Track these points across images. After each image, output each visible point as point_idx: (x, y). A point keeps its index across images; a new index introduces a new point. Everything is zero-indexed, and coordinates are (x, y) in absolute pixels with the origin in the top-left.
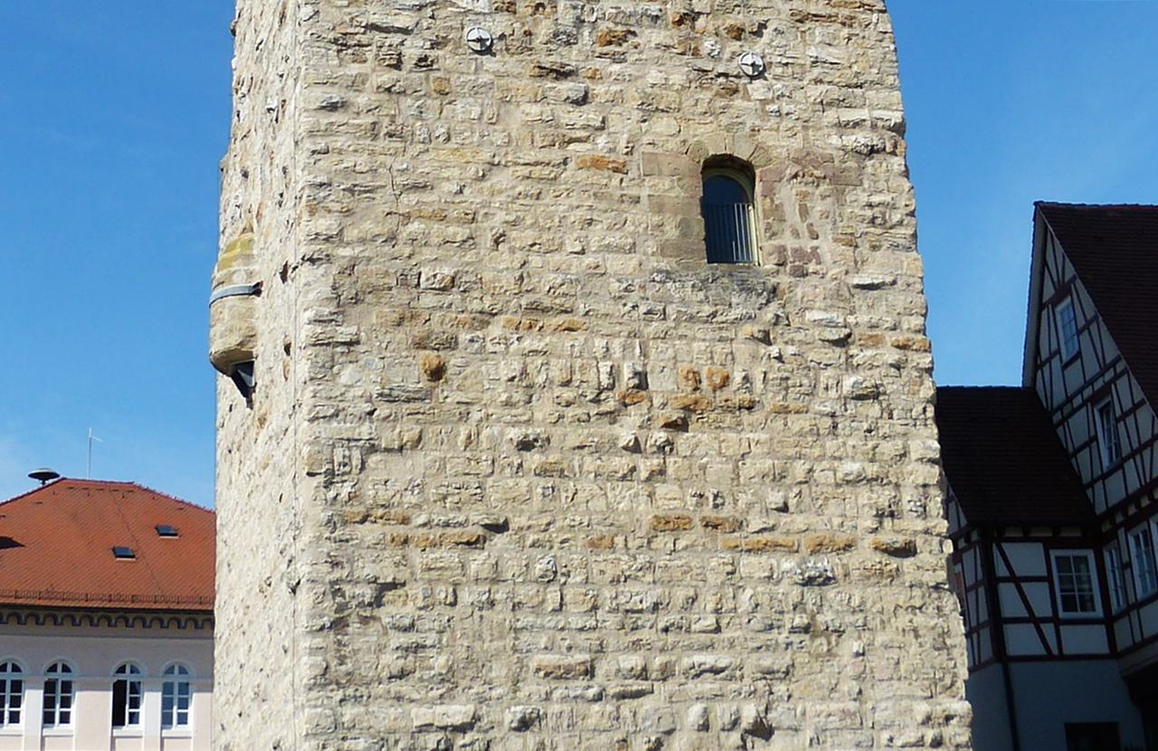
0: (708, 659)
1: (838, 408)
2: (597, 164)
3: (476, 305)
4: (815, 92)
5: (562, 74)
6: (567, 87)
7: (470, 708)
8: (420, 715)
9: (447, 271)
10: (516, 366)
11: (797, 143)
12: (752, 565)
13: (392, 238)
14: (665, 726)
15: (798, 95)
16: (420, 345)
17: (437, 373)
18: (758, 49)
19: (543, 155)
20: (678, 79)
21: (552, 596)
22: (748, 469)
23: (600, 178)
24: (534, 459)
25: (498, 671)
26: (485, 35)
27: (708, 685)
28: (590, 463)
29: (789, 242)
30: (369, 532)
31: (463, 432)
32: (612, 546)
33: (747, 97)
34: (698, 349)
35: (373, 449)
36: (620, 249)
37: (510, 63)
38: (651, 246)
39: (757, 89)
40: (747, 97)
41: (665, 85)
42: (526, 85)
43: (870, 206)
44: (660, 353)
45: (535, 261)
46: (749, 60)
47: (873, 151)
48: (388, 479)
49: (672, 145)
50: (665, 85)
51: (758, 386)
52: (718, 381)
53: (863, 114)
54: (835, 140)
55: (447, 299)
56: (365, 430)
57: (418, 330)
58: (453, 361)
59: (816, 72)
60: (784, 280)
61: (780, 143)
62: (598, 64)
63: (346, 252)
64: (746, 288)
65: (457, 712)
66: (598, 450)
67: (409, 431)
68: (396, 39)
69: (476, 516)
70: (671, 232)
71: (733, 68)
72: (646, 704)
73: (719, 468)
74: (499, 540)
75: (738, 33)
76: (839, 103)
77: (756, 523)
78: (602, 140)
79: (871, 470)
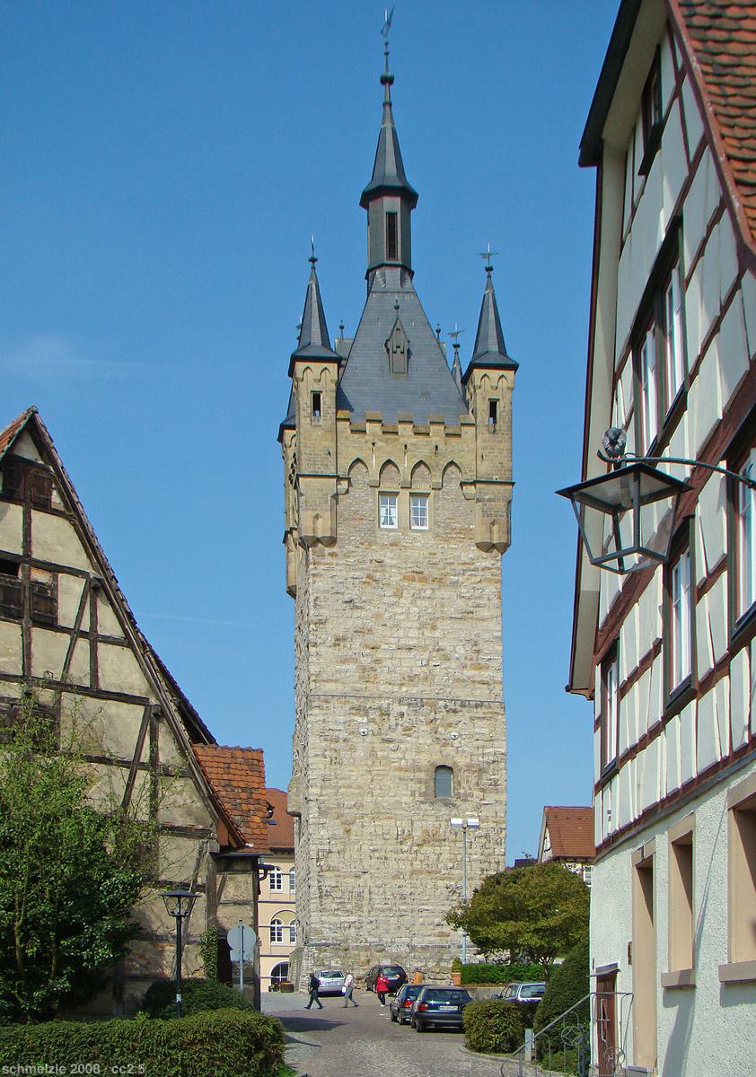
0: (426, 907)
1: (473, 840)
2: (401, 769)
3: (360, 812)
4: (476, 743)
5: (389, 741)
6: (391, 745)
7: (357, 918)
8: (342, 919)
9: (353, 803)
10: (373, 829)
11: (468, 761)
12: (440, 883)
13: (336, 794)
14: (412, 923)
15: (470, 745)
16: (344, 823)
17: (348, 831)
18: (457, 730)
19: (383, 768)
20: (429, 741)
21: (381, 890)
22: (441, 858)
23: (402, 774)
24: (377, 854)
25: (365, 909)
26: (365, 730)
27: (425, 914)
28: (395, 856)
29: (462, 791)
30: (328, 874)
31: (357, 847)
32: (399, 878)
33: (452, 746)
34: (430, 824)
35: (330, 852)
36: (406, 795)
37: (375, 739)
38: (417, 794)
39: (456, 743)
40: (452, 746)
41: (425, 743)
42: (378, 746)
43: (491, 779)
44: (417, 824)
45: (380, 799)
46: (453, 734)
47: (494, 762)
48: (334, 860)
49: (426, 763)
50: (425, 743)
51: (448, 834)
52: (435, 832)
53: (491, 750)
54: (481, 759)
55: (351, 811)
56: (327, 847)
57: (343, 819)
58: (354, 828)
59: (477, 737)
60: (458, 802)
61: (461, 761)
62: (403, 738)
63: (322, 798)
64: (446, 805)
65: (352, 918)
66: (396, 852)
67: (340, 847)
68: (337, 733)
69: (360, 869)
70: (423, 789)
71: (448, 736)
72: (407, 918)
73: (434, 857)
74: (366, 875)
75: (450, 725)
76: (483, 747)
77: (443, 871)
78: (403, 762)
79: (482, 857)
